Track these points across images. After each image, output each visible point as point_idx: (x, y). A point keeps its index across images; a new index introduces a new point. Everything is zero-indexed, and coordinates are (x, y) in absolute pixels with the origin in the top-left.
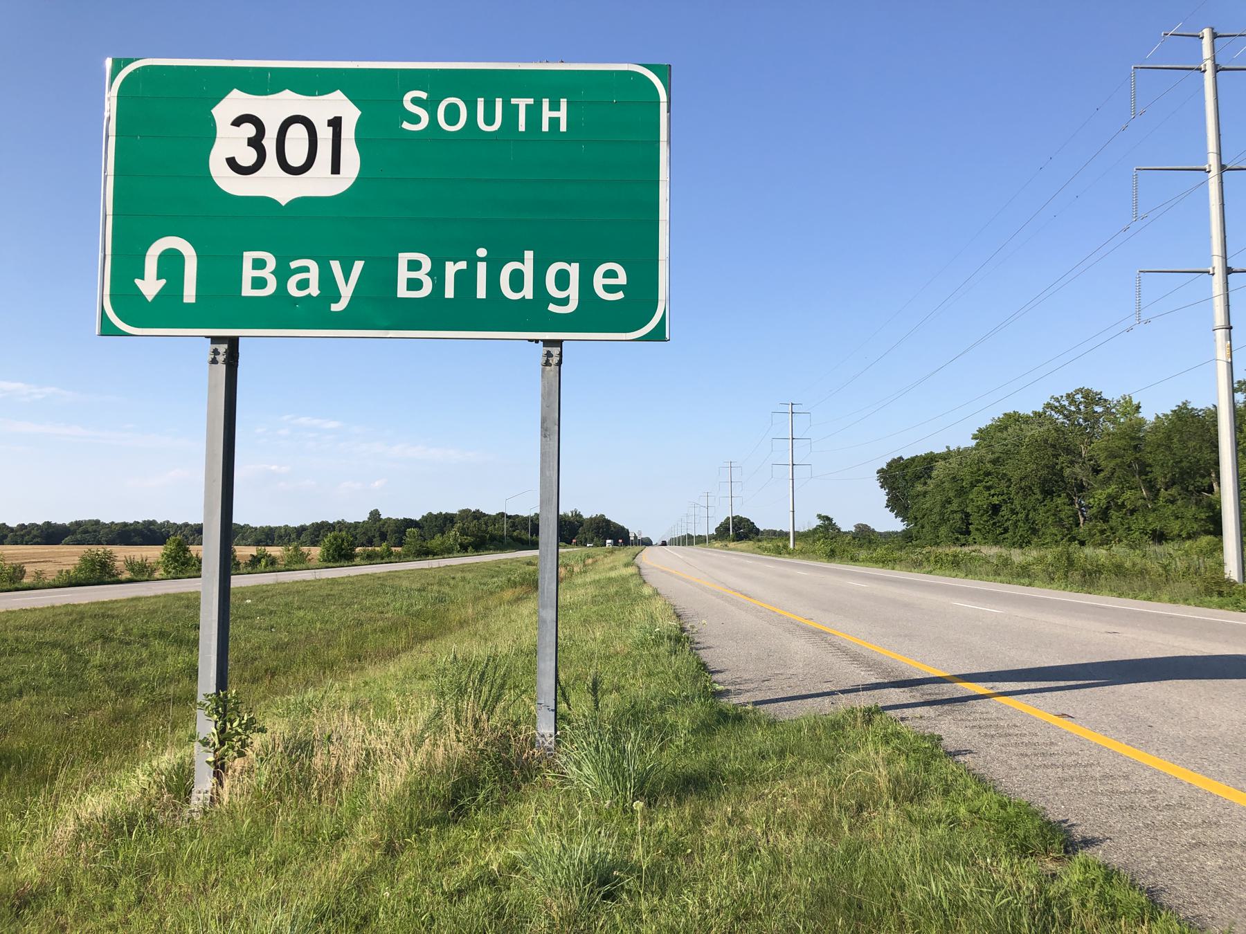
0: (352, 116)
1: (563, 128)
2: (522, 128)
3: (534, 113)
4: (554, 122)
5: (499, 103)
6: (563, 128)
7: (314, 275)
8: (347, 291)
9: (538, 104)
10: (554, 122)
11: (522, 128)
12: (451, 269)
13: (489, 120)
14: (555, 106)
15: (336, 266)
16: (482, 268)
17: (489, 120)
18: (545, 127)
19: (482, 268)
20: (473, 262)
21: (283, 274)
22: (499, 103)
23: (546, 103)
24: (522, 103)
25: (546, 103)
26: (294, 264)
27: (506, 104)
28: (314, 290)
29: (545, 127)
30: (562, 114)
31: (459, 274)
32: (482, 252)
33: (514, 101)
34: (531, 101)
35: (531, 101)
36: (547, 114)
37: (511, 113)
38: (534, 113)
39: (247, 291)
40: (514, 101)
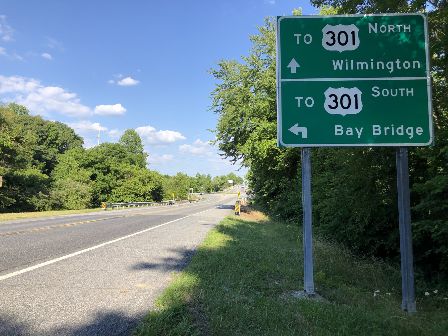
0: (359, 93)
1: (412, 95)
2: (402, 95)
3: (405, 92)
4: (410, 94)
5: (396, 90)
6: (412, 95)
7: (351, 131)
8: (359, 134)
9: (406, 90)
10: (410, 94)
11: (402, 95)
12: (386, 129)
13: (394, 93)
14: (410, 90)
15: (356, 128)
16: (393, 128)
17: (394, 93)
18: (407, 95)
19: (393, 128)
20: (391, 127)
21: (345, 130)
22: (396, 90)
23: (407, 89)
24: (402, 90)
25: (407, 89)
26: (347, 129)
27: (398, 90)
28: (351, 134)
29: (407, 95)
30: (412, 92)
31: (387, 130)
32: (392, 125)
33: (400, 89)
34: (404, 89)
35: (404, 89)
36: (408, 92)
37: (399, 92)
38: (405, 92)
39: (336, 134)
40: (400, 89)
